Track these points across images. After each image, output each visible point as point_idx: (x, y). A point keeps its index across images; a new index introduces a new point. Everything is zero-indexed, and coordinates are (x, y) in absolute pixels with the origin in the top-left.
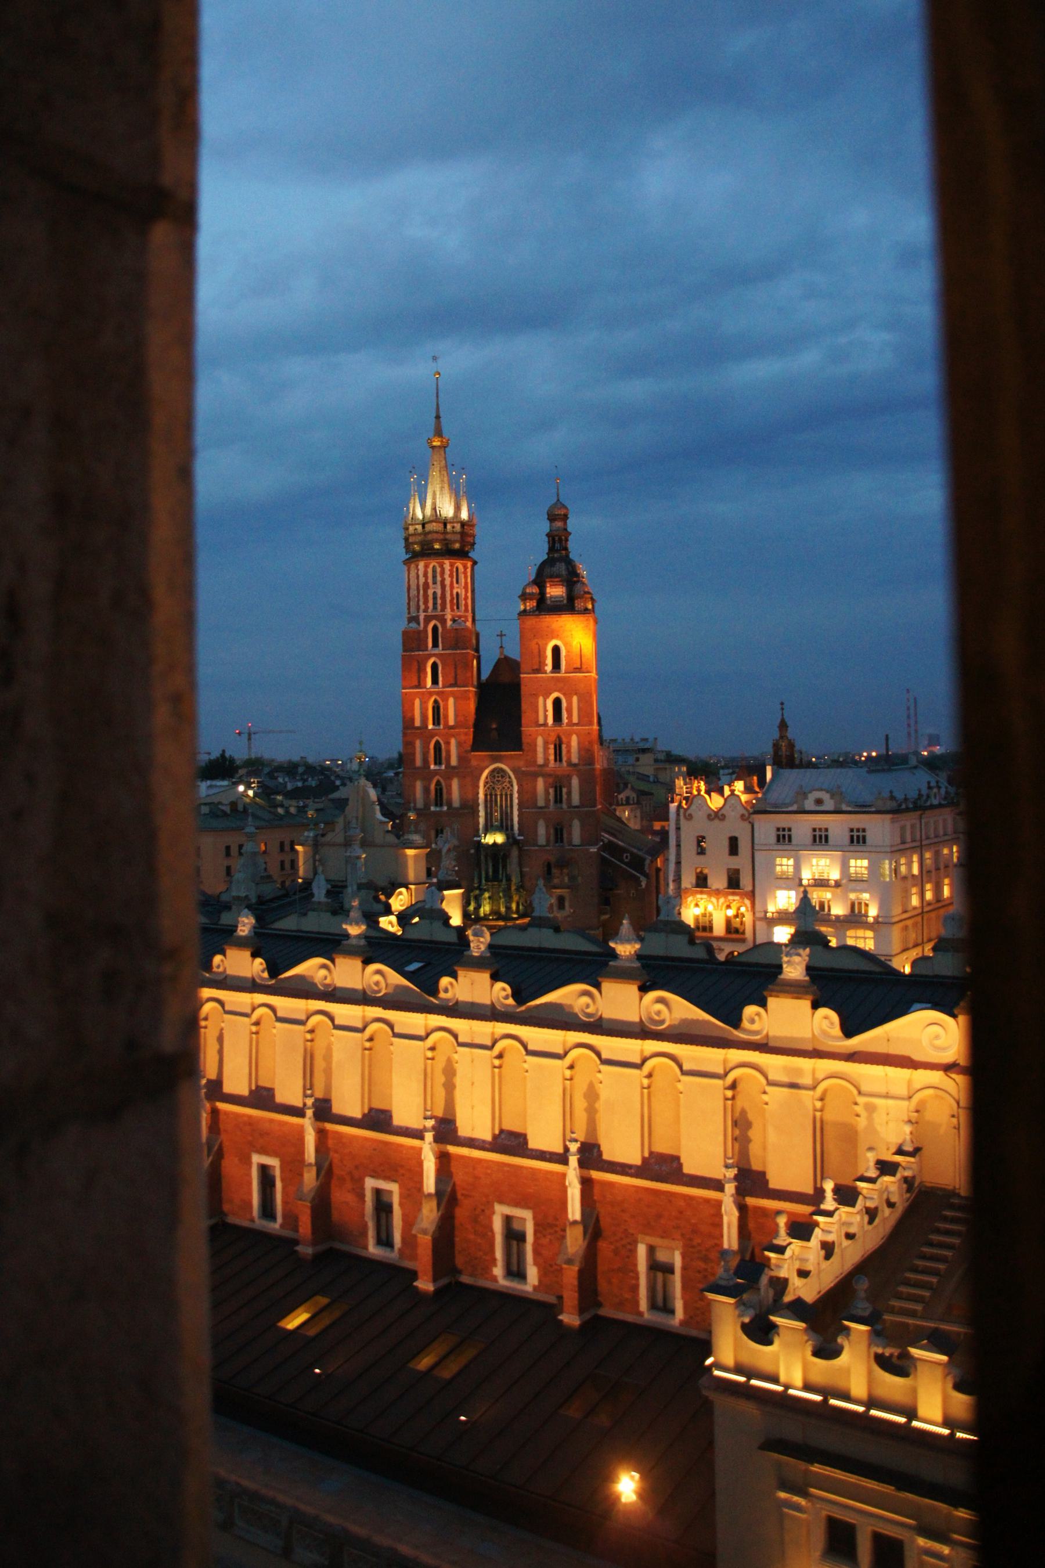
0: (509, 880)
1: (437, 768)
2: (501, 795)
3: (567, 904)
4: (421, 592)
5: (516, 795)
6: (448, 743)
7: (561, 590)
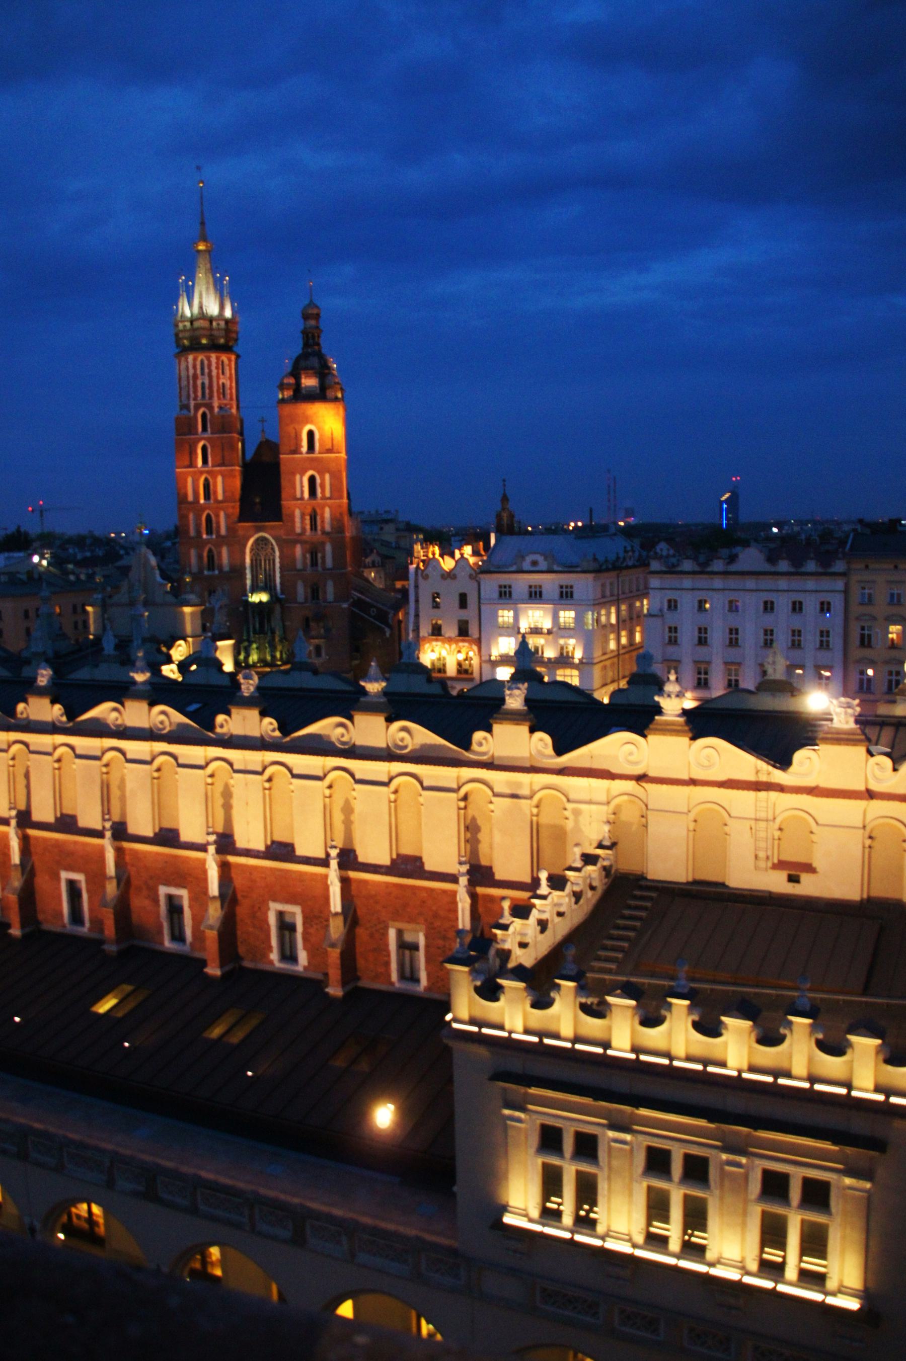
0: (273, 632)
4: (191, 382)
6: (218, 516)
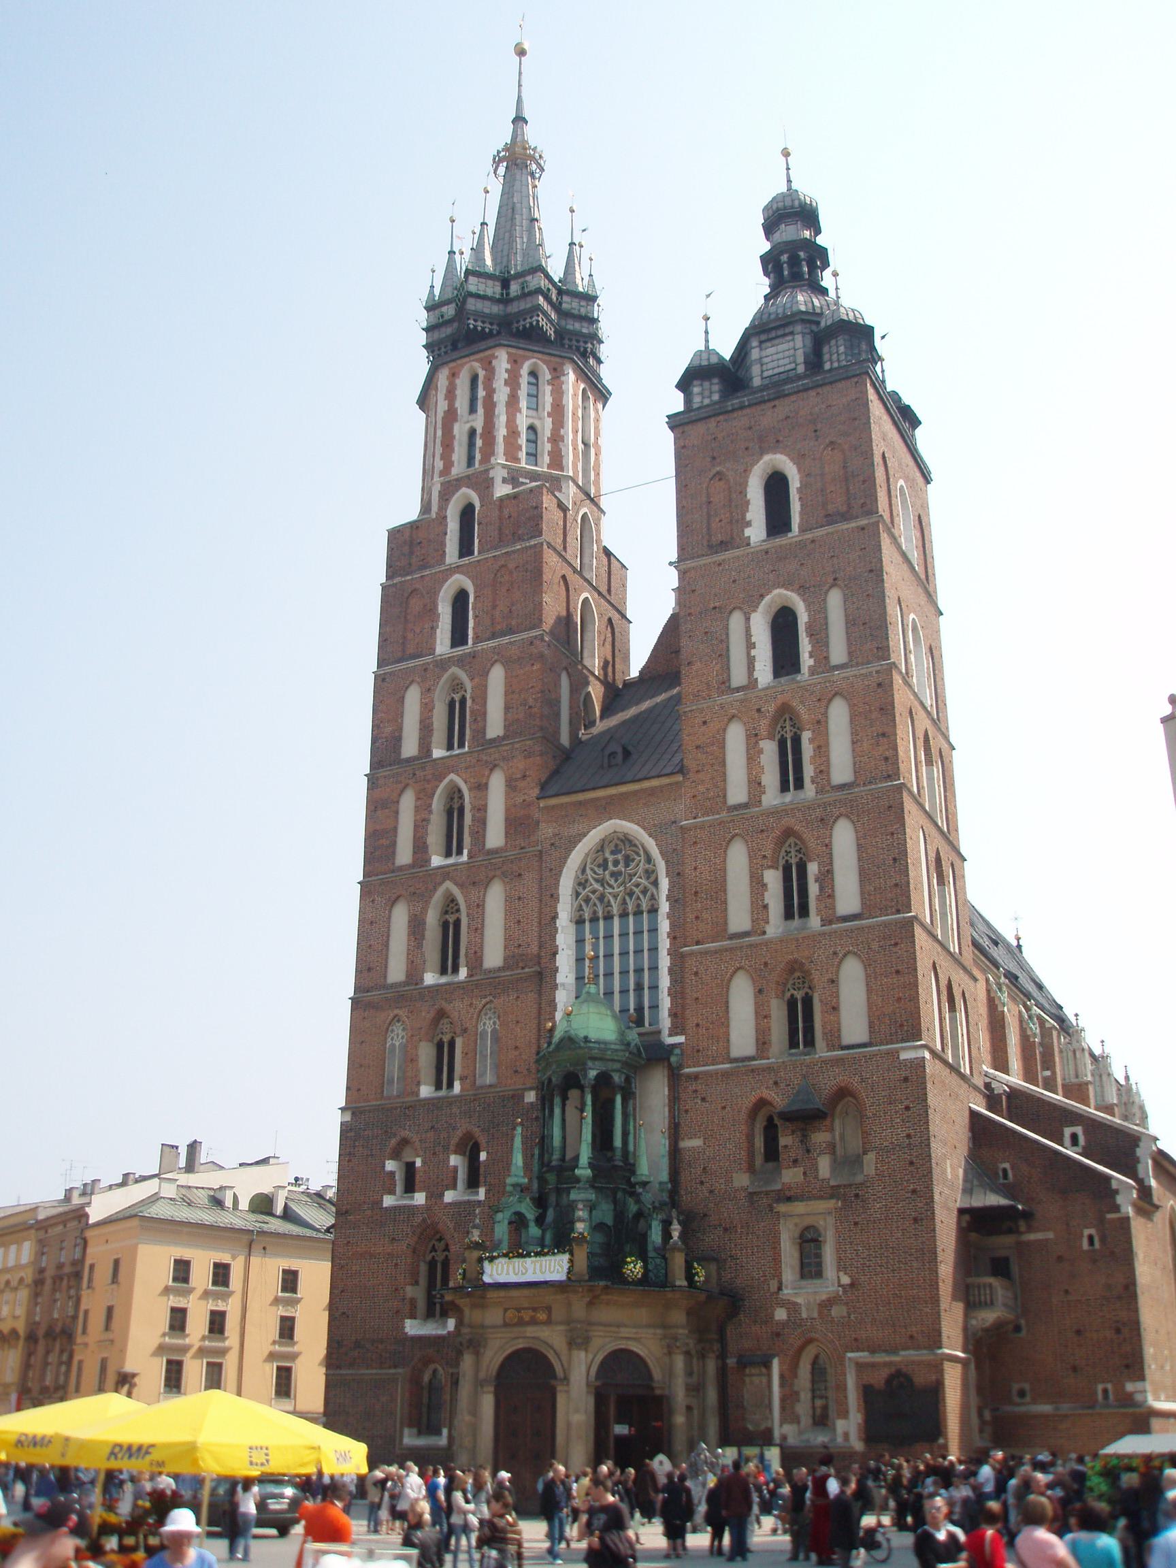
1: (451, 861)
2: (624, 915)
3: (829, 1254)
4: (439, 433)
5: (664, 907)
6: (481, 788)
7: (791, 344)
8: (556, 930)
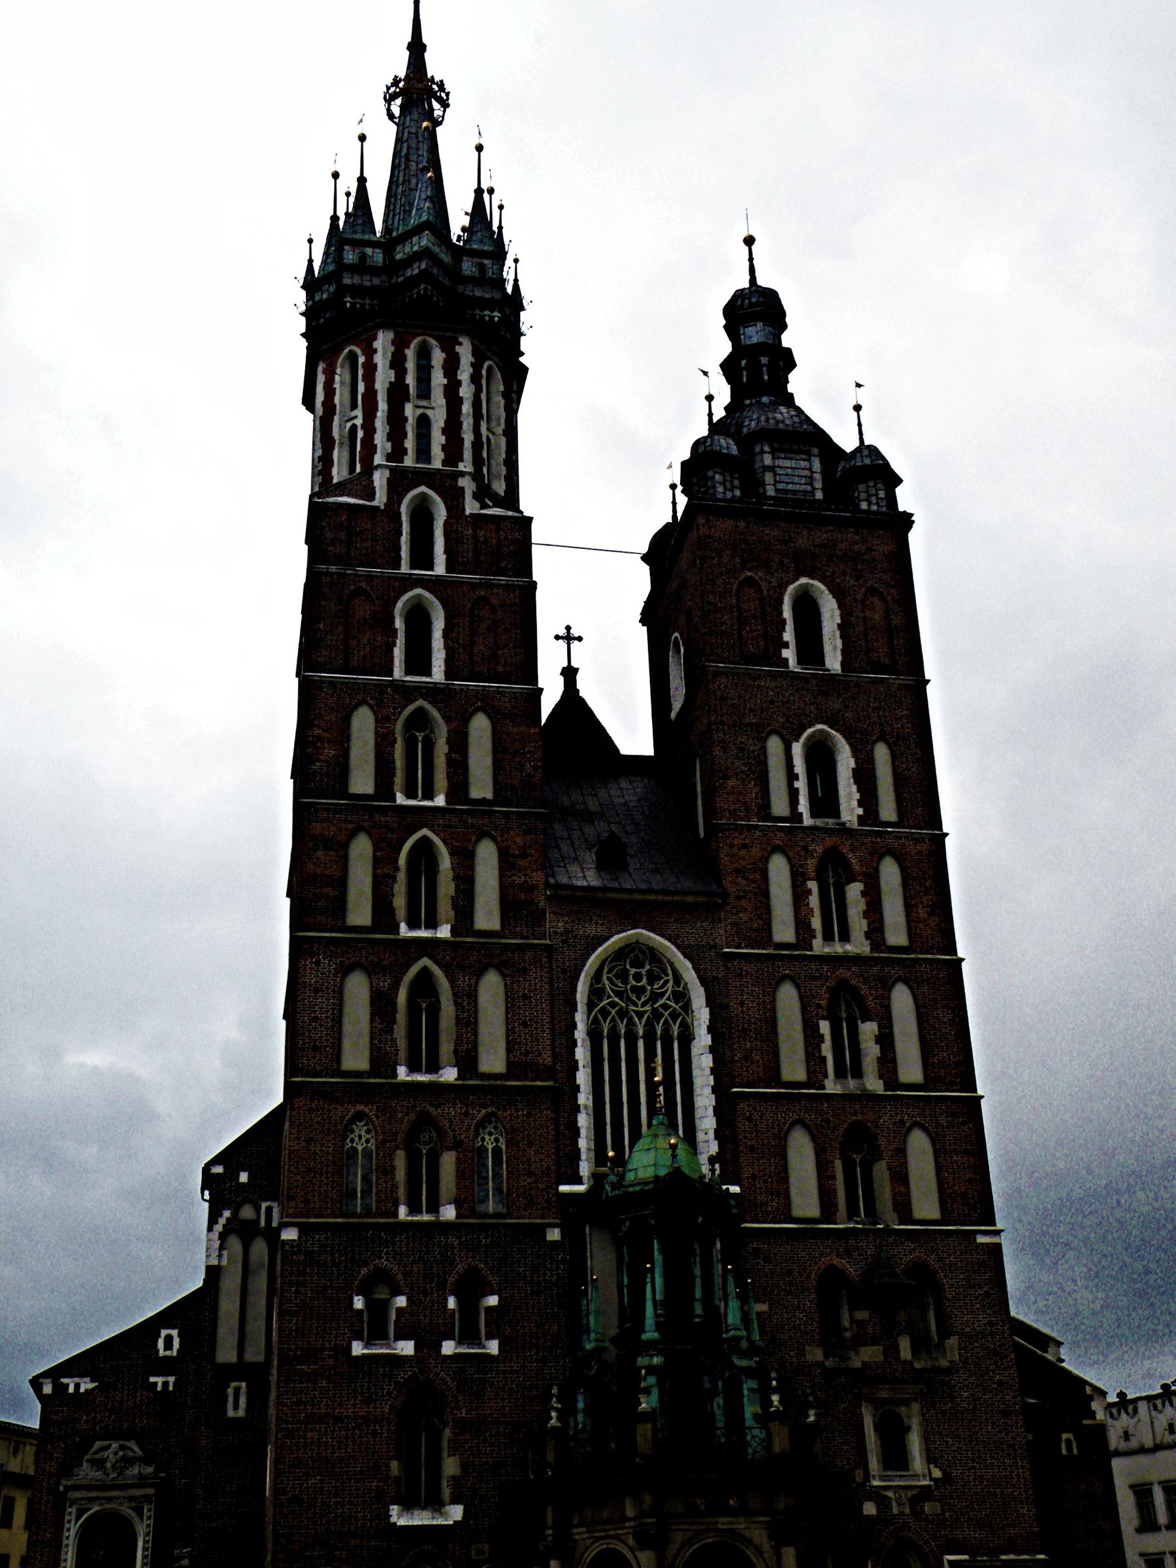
8: (574, 1043)
